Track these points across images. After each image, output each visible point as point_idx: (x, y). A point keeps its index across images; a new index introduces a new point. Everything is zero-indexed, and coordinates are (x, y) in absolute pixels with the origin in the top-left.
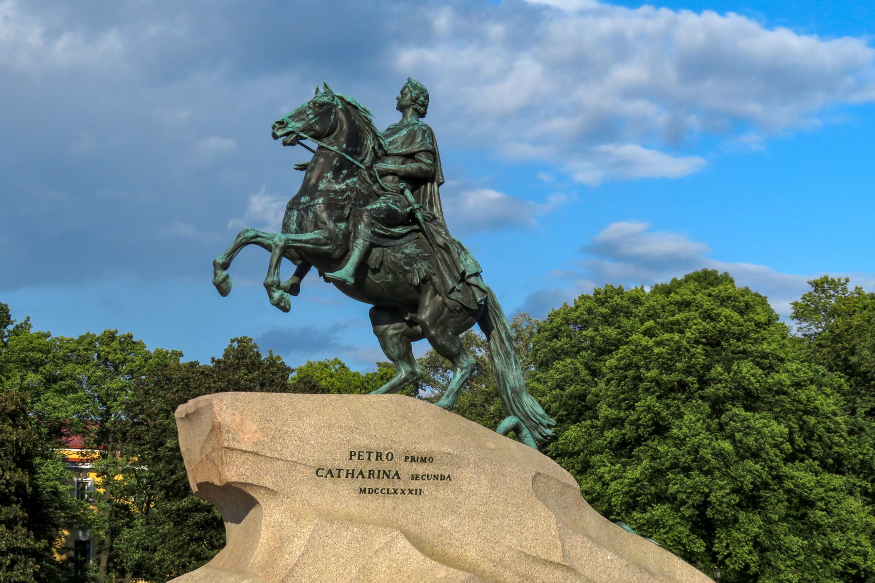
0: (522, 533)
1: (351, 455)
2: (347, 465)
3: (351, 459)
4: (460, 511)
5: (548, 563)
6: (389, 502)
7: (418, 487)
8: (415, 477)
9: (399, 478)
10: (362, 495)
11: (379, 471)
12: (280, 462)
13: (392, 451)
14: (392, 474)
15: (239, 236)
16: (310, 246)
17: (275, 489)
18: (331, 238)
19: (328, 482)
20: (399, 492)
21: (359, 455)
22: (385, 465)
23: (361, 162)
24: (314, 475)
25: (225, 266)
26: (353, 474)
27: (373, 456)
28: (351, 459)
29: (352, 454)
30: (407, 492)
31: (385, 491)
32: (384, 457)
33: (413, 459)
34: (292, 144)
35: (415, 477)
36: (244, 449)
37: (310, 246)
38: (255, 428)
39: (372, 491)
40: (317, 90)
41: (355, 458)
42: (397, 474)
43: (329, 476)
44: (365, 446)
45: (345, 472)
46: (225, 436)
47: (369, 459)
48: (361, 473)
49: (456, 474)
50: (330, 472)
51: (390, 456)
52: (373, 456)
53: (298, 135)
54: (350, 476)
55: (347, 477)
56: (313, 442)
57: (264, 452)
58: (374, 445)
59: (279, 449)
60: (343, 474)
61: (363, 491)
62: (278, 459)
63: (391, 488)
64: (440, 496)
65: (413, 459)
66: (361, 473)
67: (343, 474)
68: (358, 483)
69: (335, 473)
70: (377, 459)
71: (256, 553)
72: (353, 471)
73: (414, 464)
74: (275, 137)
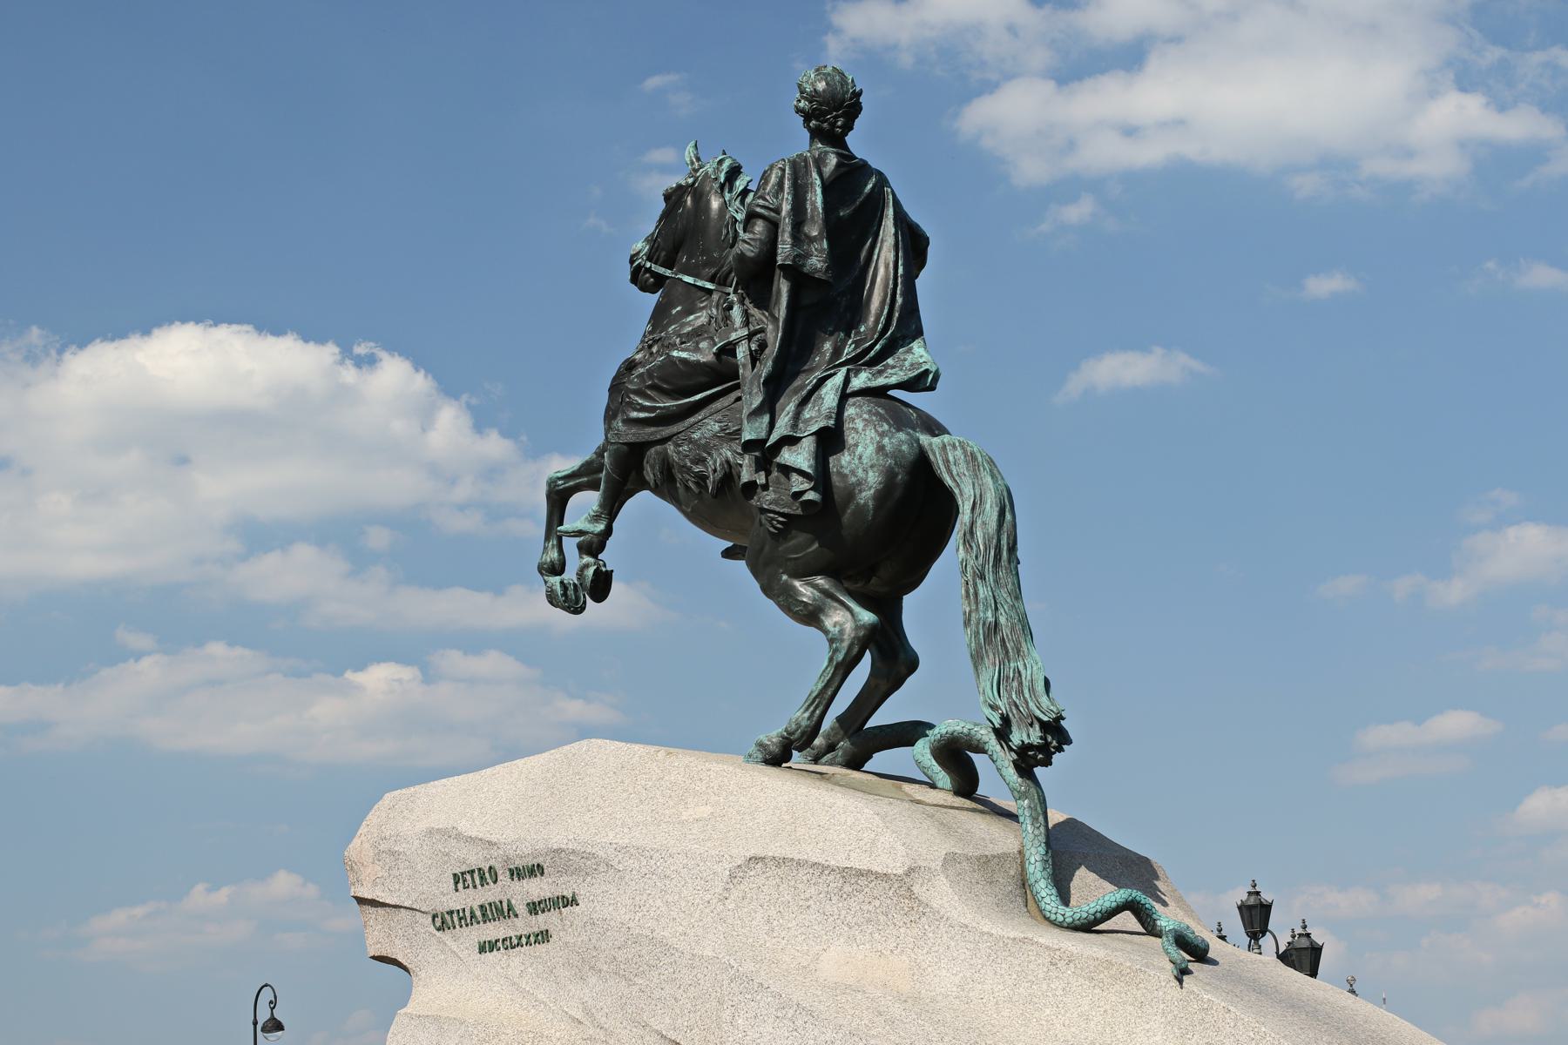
1: (456, 883)
7: (543, 928)
8: (534, 908)
13: (492, 862)
19: (446, 936)
22: (489, 894)
23: (712, 280)
24: (432, 929)
27: (476, 875)
33: (516, 874)
35: (534, 908)
41: (460, 885)
48: (472, 912)
49: (583, 893)
52: (476, 875)
61: (482, 950)
63: (512, 934)
66: (473, 916)
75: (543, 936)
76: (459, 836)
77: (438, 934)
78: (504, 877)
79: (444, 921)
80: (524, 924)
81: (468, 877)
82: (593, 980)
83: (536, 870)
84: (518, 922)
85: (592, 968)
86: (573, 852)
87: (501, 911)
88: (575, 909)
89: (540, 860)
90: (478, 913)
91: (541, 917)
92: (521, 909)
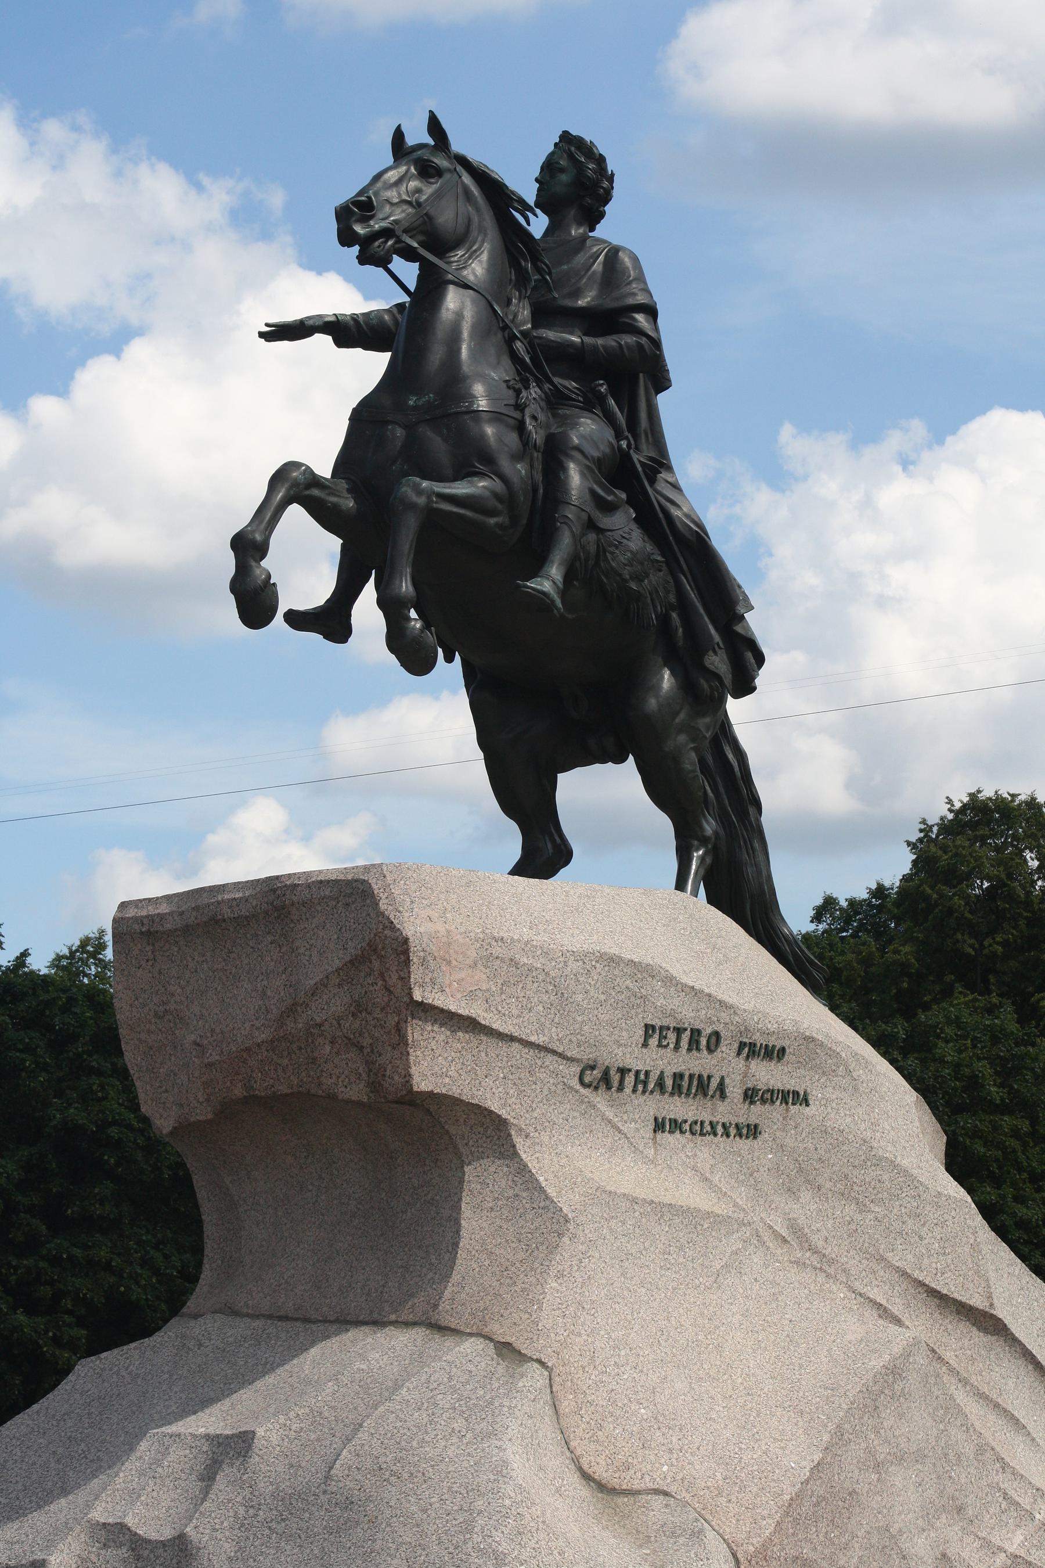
0: (921, 1238)
1: (647, 1036)
2: (638, 1059)
3: (645, 1045)
4: (820, 1180)
5: (965, 1311)
6: (704, 1152)
7: (753, 1120)
8: (750, 1095)
9: (723, 1096)
10: (659, 1135)
11: (691, 1076)
12: (516, 1045)
13: (720, 1028)
14: (714, 1083)
15: (277, 479)
16: (469, 513)
17: (503, 1113)
18: (508, 499)
19: (600, 1099)
20: (720, 1130)
21: (663, 1037)
24: (575, 1083)
25: (262, 550)
26: (645, 1083)
27: (686, 1037)
28: (645, 1045)
29: (649, 1029)
30: (733, 1131)
31: (698, 1128)
32: (703, 1042)
34: (383, 262)
35: (750, 1095)
36: (453, 1008)
37: (469, 513)
38: (472, 954)
39: (676, 1126)
40: (398, 136)
41: (654, 1042)
42: (721, 1087)
43: (602, 1086)
44: (672, 1014)
45: (632, 1075)
46: (416, 974)
47: (677, 1047)
50: (606, 1073)
51: (713, 1040)
52: (686, 1037)
53: (399, 241)
54: (640, 1087)
55: (634, 1091)
56: (579, 997)
57: (486, 1018)
58: (689, 1015)
59: (515, 1012)
60: (630, 1080)
61: (659, 1126)
62: (512, 1039)
63: (706, 1117)
64: (789, 1142)
65: (750, 1050)
67: (630, 1080)
68: (654, 1106)
69: (615, 1078)
70: (689, 1050)
71: (455, 1277)
72: (647, 1073)
73: (754, 1063)
74: (346, 238)
75: (753, 1131)
76: (669, 980)
77: (583, 1091)
78: (727, 1049)
79: (604, 1079)
80: (731, 1110)
81: (672, 1037)
82: (805, 1196)
83: (774, 1053)
84: (722, 1107)
85: (808, 1181)
86: (822, 1045)
87: (701, 1086)
88: (803, 1109)
89: (786, 1043)
90: (669, 1082)
91: (757, 1108)
92: (735, 1091)
